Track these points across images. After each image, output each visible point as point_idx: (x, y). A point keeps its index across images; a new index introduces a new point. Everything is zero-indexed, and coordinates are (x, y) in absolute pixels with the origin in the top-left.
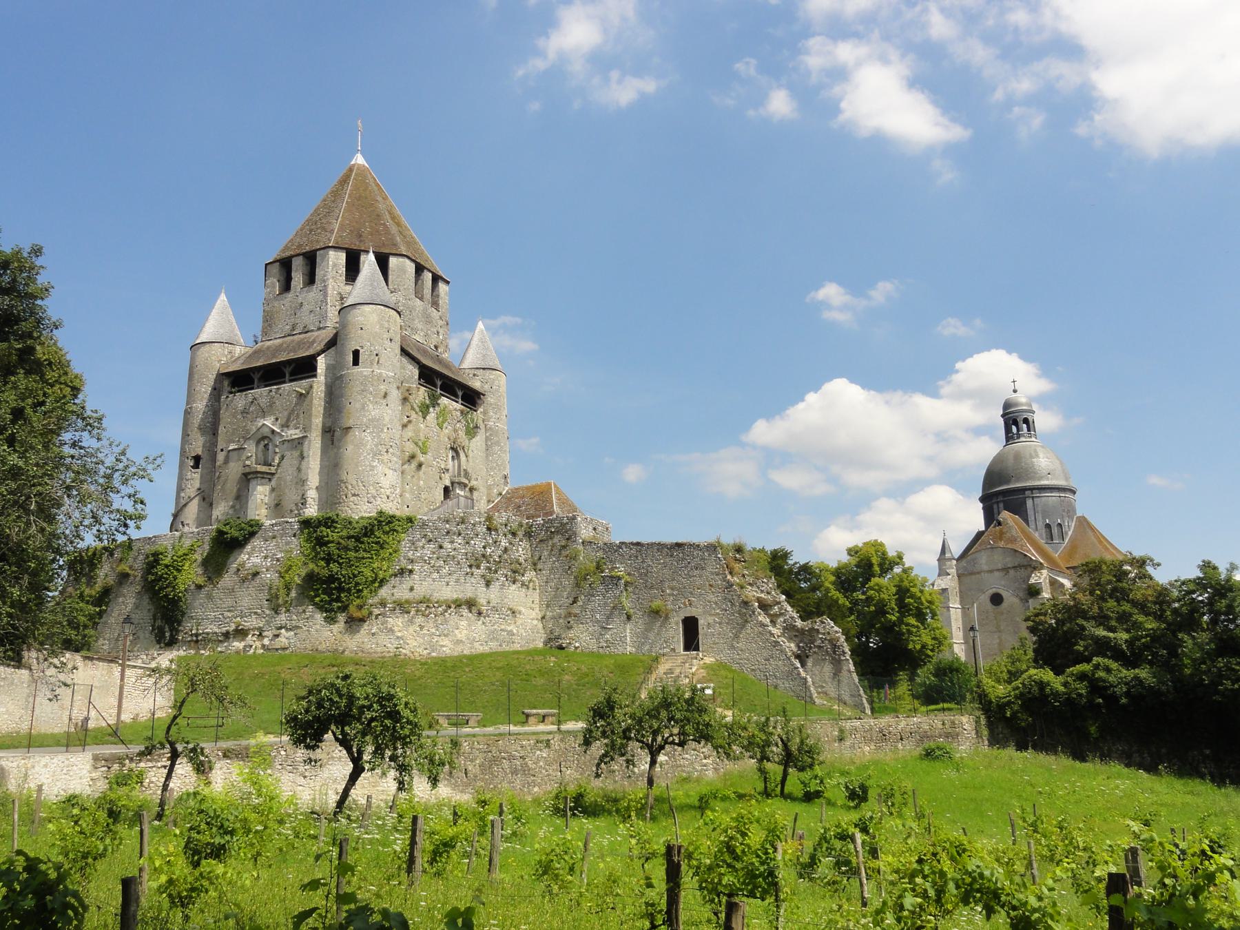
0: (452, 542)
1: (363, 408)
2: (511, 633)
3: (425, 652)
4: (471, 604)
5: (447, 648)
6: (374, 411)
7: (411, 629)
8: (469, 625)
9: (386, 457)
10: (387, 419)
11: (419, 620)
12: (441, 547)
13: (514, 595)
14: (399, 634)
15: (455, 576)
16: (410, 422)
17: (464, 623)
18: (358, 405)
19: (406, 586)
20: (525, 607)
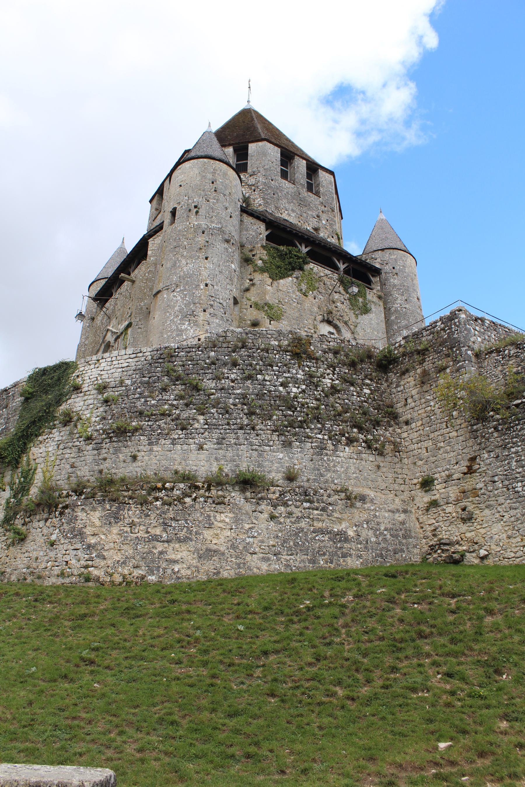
0: (217, 378)
1: (174, 265)
2: (341, 537)
3: (137, 573)
4: (247, 483)
5: (183, 562)
6: (187, 266)
7: (115, 530)
8: (237, 520)
9: (202, 317)
10: (205, 273)
11: (132, 513)
12: (196, 388)
13: (349, 465)
14: (93, 541)
15: (215, 435)
16: (253, 285)
17: (226, 517)
18: (169, 265)
19: (125, 453)
20: (376, 489)
